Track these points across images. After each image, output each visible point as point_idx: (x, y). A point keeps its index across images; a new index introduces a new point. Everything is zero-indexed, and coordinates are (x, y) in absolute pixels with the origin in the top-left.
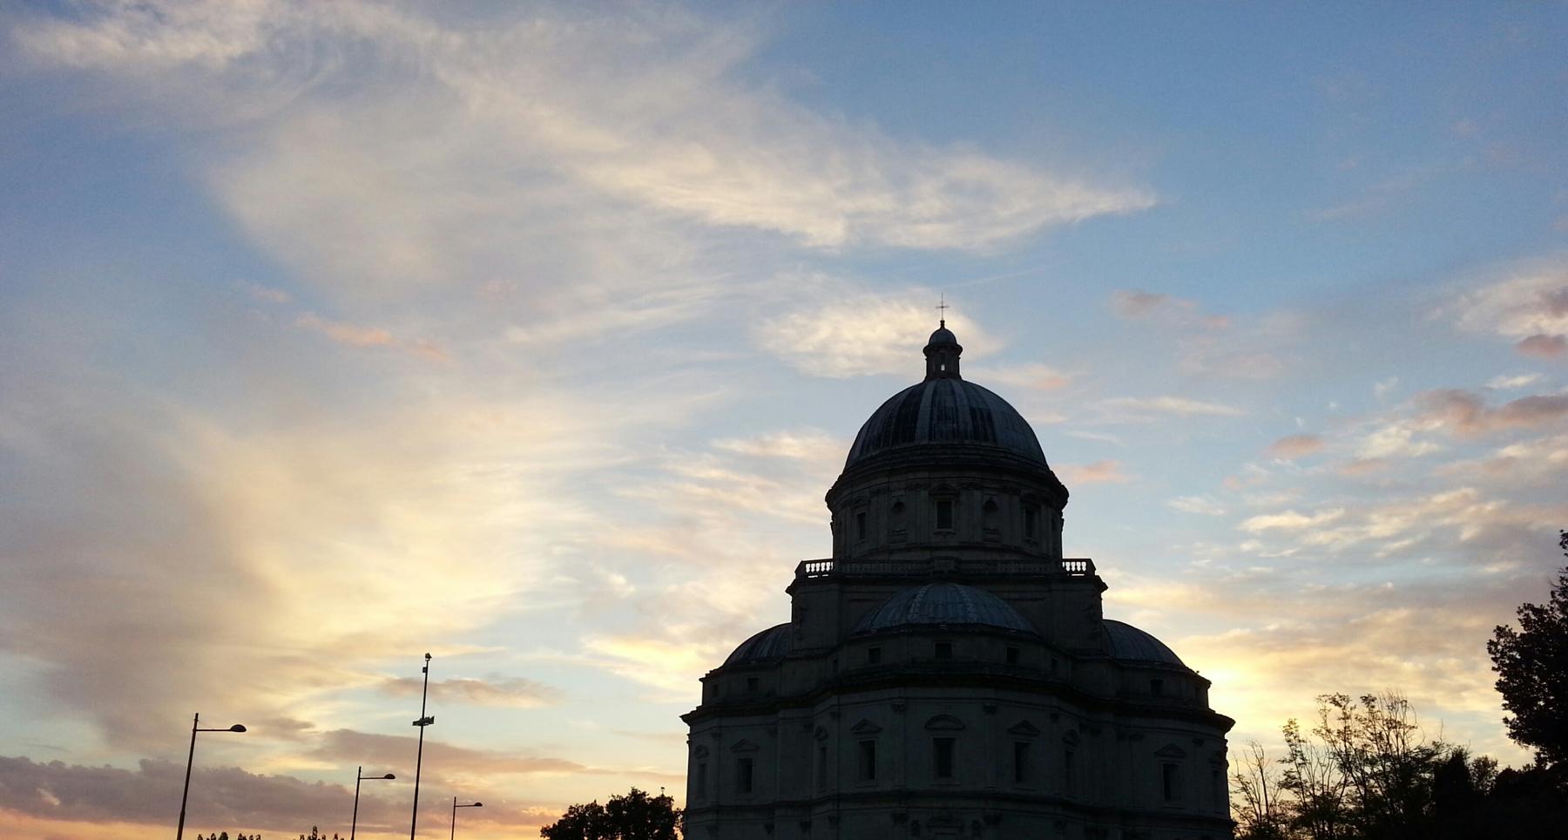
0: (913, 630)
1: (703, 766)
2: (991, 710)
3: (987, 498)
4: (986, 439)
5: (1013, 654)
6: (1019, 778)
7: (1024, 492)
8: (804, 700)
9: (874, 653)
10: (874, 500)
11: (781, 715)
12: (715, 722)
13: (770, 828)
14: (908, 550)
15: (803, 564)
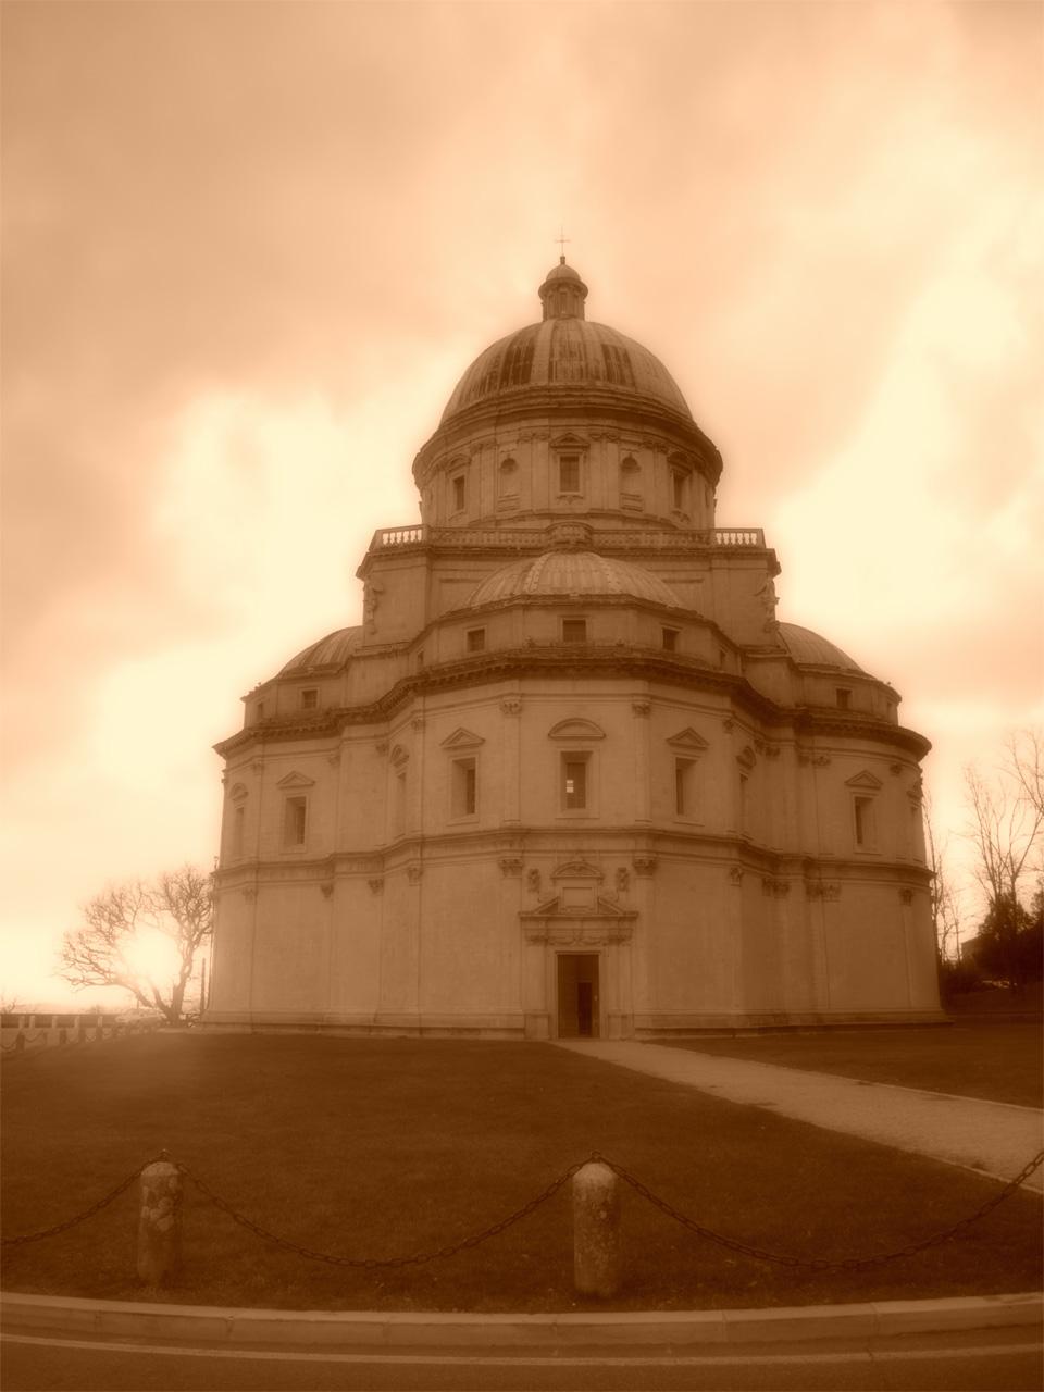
0: (529, 603)
1: (241, 811)
2: (644, 711)
3: (625, 454)
4: (622, 382)
5: (670, 636)
6: (680, 809)
7: (671, 451)
8: (381, 711)
9: (476, 637)
10: (476, 458)
11: (345, 734)
12: (258, 750)
13: (328, 891)
14: (522, 518)
15: (379, 533)
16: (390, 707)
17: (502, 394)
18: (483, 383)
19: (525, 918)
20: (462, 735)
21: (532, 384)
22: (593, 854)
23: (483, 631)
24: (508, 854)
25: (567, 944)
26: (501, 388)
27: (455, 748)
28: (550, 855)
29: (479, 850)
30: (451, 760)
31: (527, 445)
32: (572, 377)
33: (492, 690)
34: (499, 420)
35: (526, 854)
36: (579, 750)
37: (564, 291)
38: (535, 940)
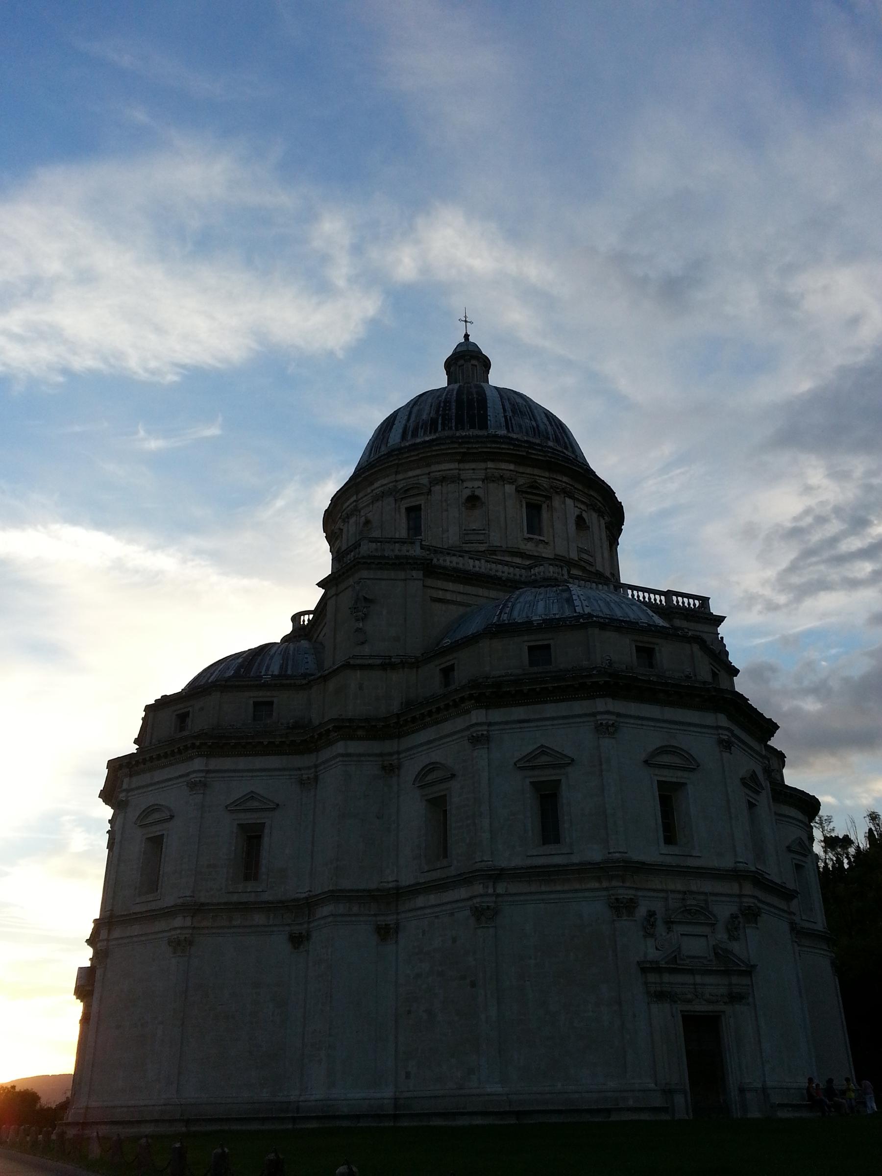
2: (726, 745)
10: (437, 488)
16: (414, 719)
17: (458, 434)
18: (433, 423)
19: (646, 968)
20: (543, 753)
21: (492, 431)
22: (702, 897)
23: (548, 647)
24: (620, 891)
25: (689, 1001)
26: (457, 429)
27: (533, 768)
28: (661, 895)
29: (577, 886)
30: (528, 781)
31: (492, 486)
32: (527, 433)
33: (579, 707)
34: (465, 458)
35: (640, 893)
36: (674, 780)
37: (468, 361)
38: (661, 996)
